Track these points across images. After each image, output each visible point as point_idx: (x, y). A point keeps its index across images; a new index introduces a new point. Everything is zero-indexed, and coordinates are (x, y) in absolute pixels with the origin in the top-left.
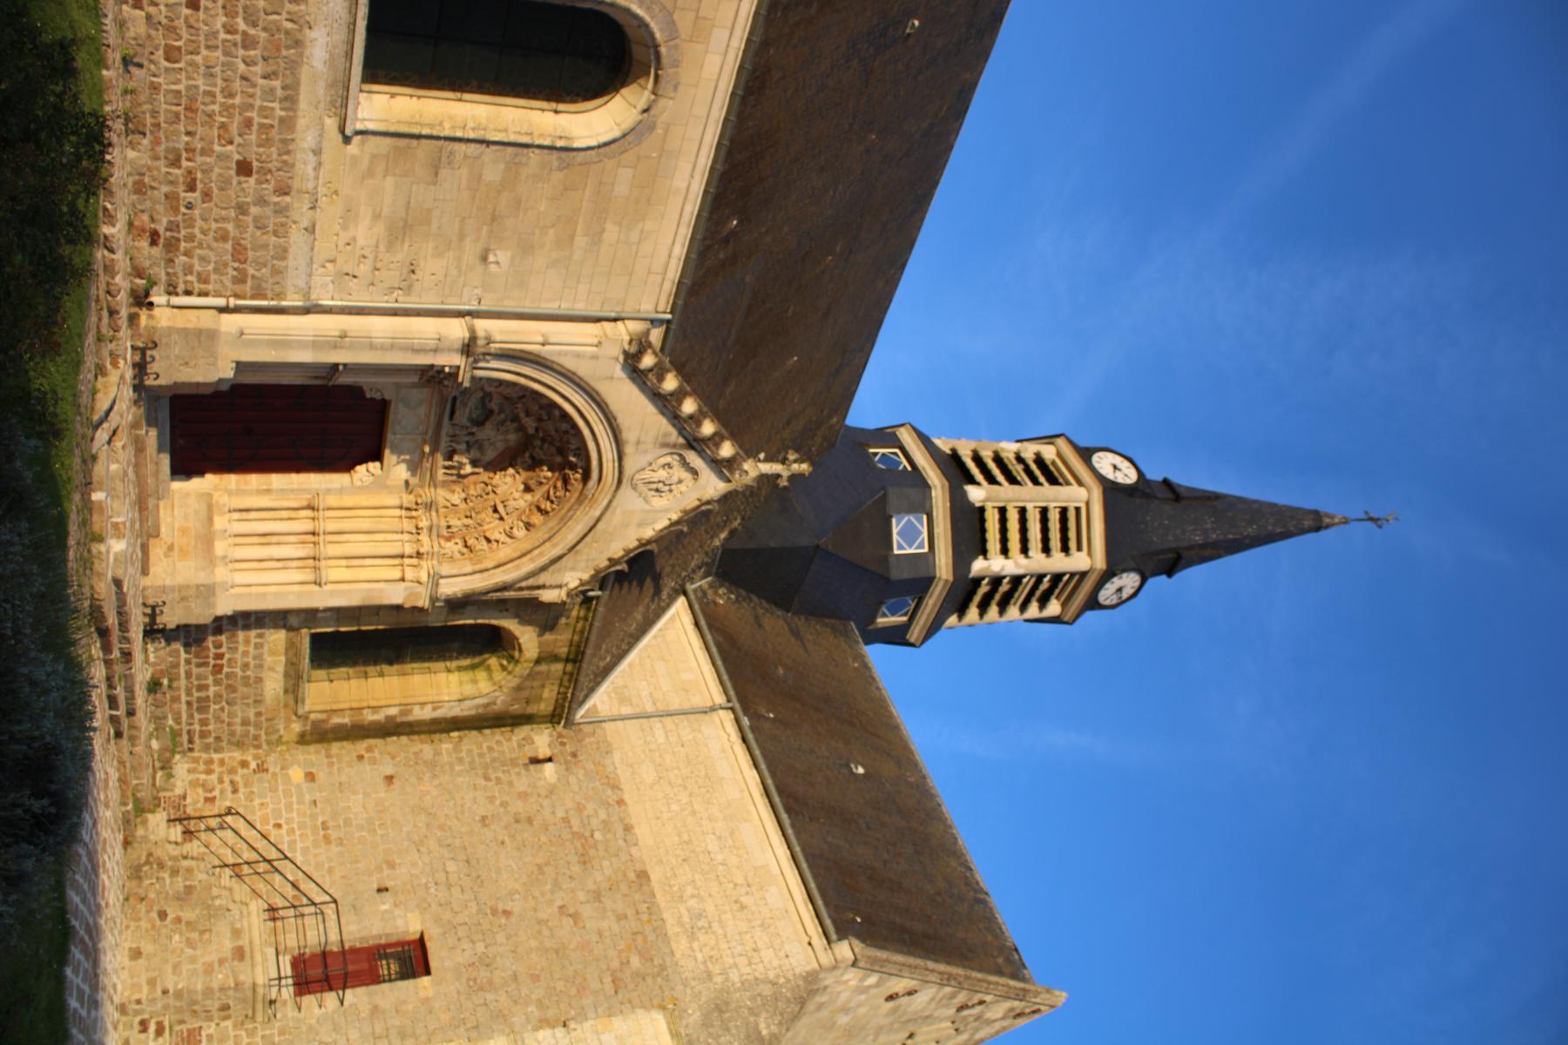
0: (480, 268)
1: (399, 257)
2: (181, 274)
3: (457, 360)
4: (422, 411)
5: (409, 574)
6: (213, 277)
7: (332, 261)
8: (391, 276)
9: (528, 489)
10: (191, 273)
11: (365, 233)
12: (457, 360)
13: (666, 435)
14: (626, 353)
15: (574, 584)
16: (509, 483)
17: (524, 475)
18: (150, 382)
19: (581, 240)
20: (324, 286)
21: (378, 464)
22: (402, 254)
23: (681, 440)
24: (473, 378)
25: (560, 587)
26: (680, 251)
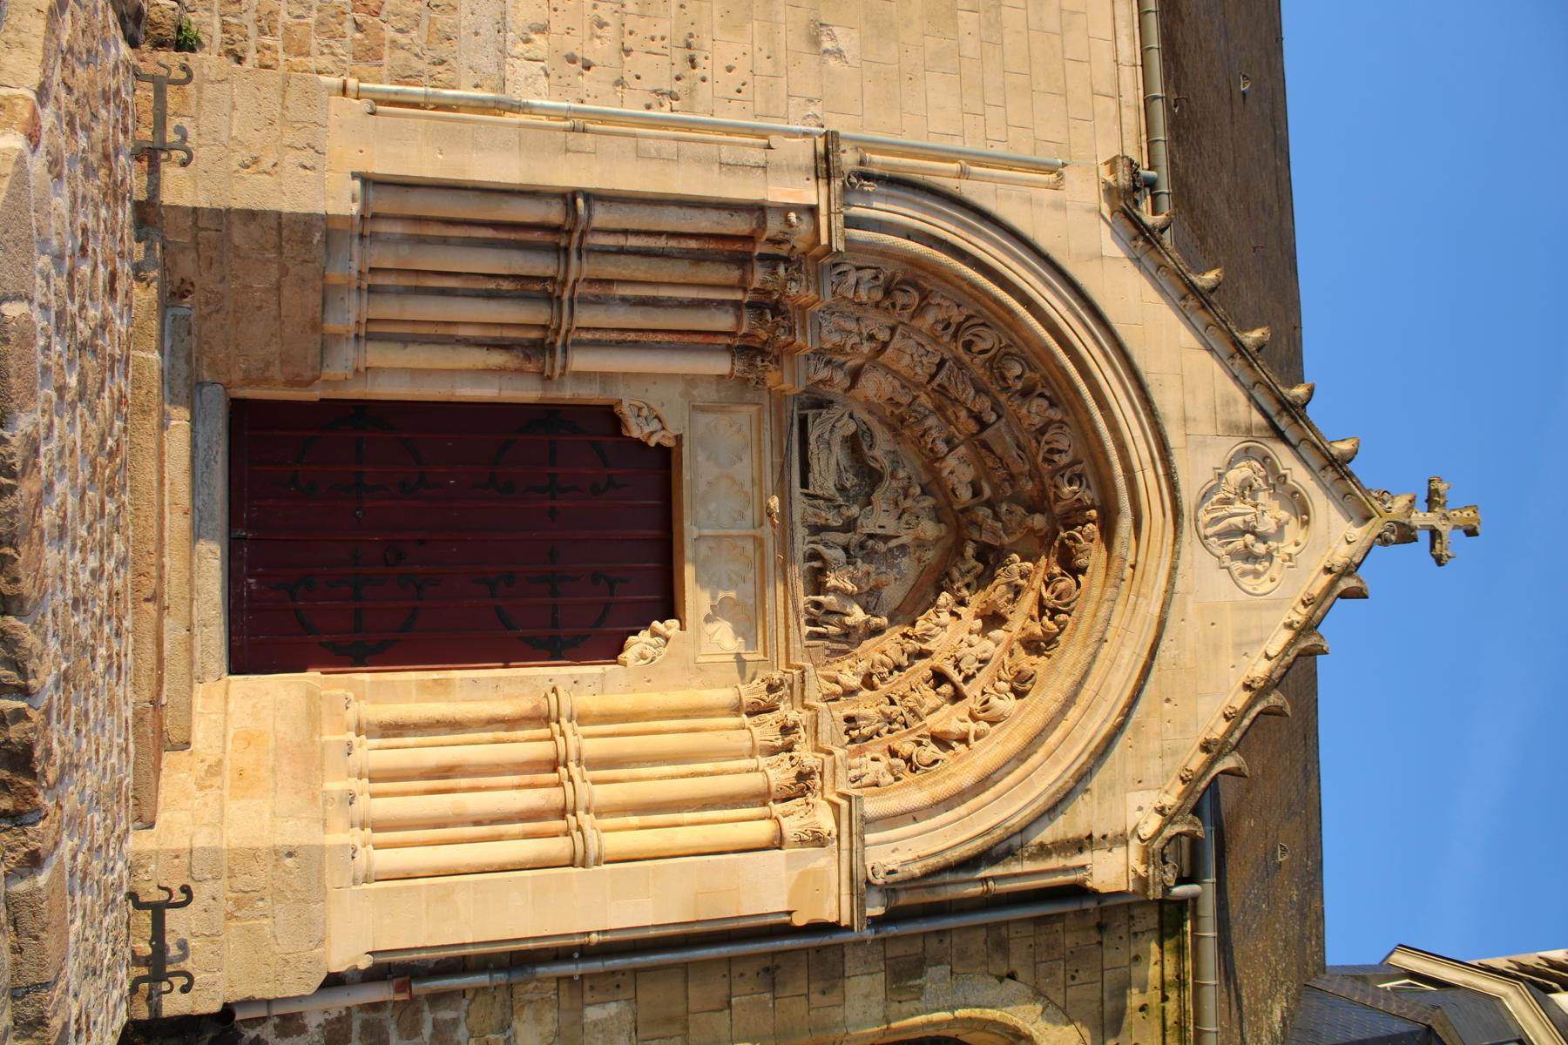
0: (810, 61)
2: (252, 31)
3: (808, 193)
4: (744, 470)
5: (792, 827)
6: (314, 42)
7: (542, 29)
8: (656, 71)
9: (993, 619)
10: (271, 31)
12: (808, 193)
13: (1228, 402)
14: (1110, 191)
15: (1150, 825)
16: (951, 632)
17: (976, 601)
18: (181, 188)
19: (967, 21)
20: (530, 79)
21: (674, 623)
23: (1257, 418)
24: (848, 241)
25: (1122, 839)
26: (1128, 49)
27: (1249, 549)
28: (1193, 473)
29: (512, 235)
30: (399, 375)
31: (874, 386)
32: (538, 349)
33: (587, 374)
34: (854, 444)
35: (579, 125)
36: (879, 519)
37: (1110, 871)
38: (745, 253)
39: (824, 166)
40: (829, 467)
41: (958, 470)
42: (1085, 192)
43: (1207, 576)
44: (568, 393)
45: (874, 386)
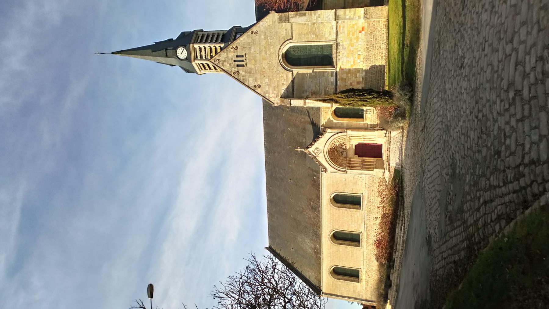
1: (355, 180)
11: (359, 183)
22: (355, 180)
27: (317, 149)
28: (322, 154)
29: (365, 168)
30: (372, 159)
31: (342, 158)
32: (363, 161)
33: (360, 159)
34: (342, 155)
35: (361, 174)
36: (341, 150)
37: (329, 130)
38: (352, 167)
39: (347, 172)
40: (344, 153)
41: (336, 153)
42: (329, 171)
43: (321, 148)
44: (361, 158)
45: (342, 158)
